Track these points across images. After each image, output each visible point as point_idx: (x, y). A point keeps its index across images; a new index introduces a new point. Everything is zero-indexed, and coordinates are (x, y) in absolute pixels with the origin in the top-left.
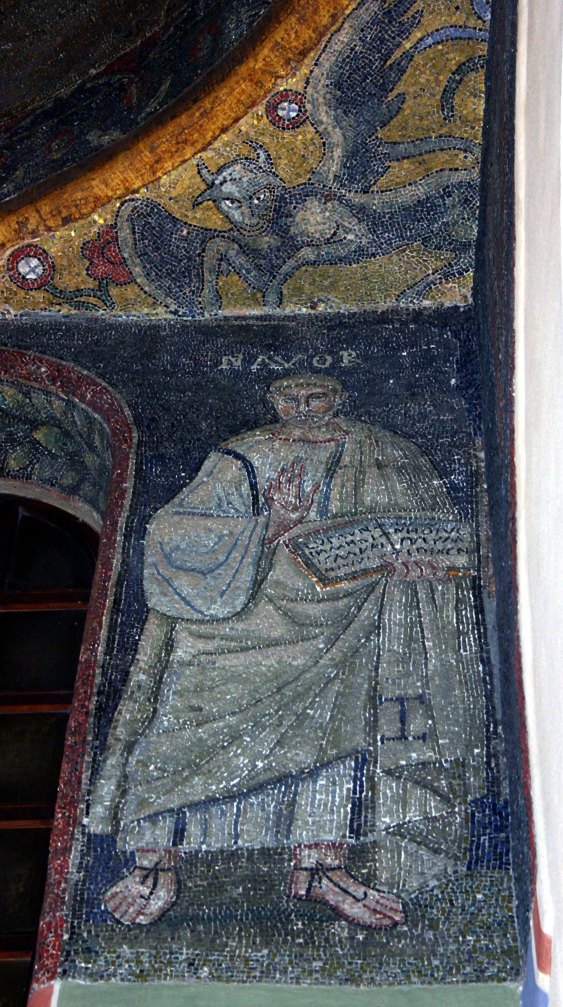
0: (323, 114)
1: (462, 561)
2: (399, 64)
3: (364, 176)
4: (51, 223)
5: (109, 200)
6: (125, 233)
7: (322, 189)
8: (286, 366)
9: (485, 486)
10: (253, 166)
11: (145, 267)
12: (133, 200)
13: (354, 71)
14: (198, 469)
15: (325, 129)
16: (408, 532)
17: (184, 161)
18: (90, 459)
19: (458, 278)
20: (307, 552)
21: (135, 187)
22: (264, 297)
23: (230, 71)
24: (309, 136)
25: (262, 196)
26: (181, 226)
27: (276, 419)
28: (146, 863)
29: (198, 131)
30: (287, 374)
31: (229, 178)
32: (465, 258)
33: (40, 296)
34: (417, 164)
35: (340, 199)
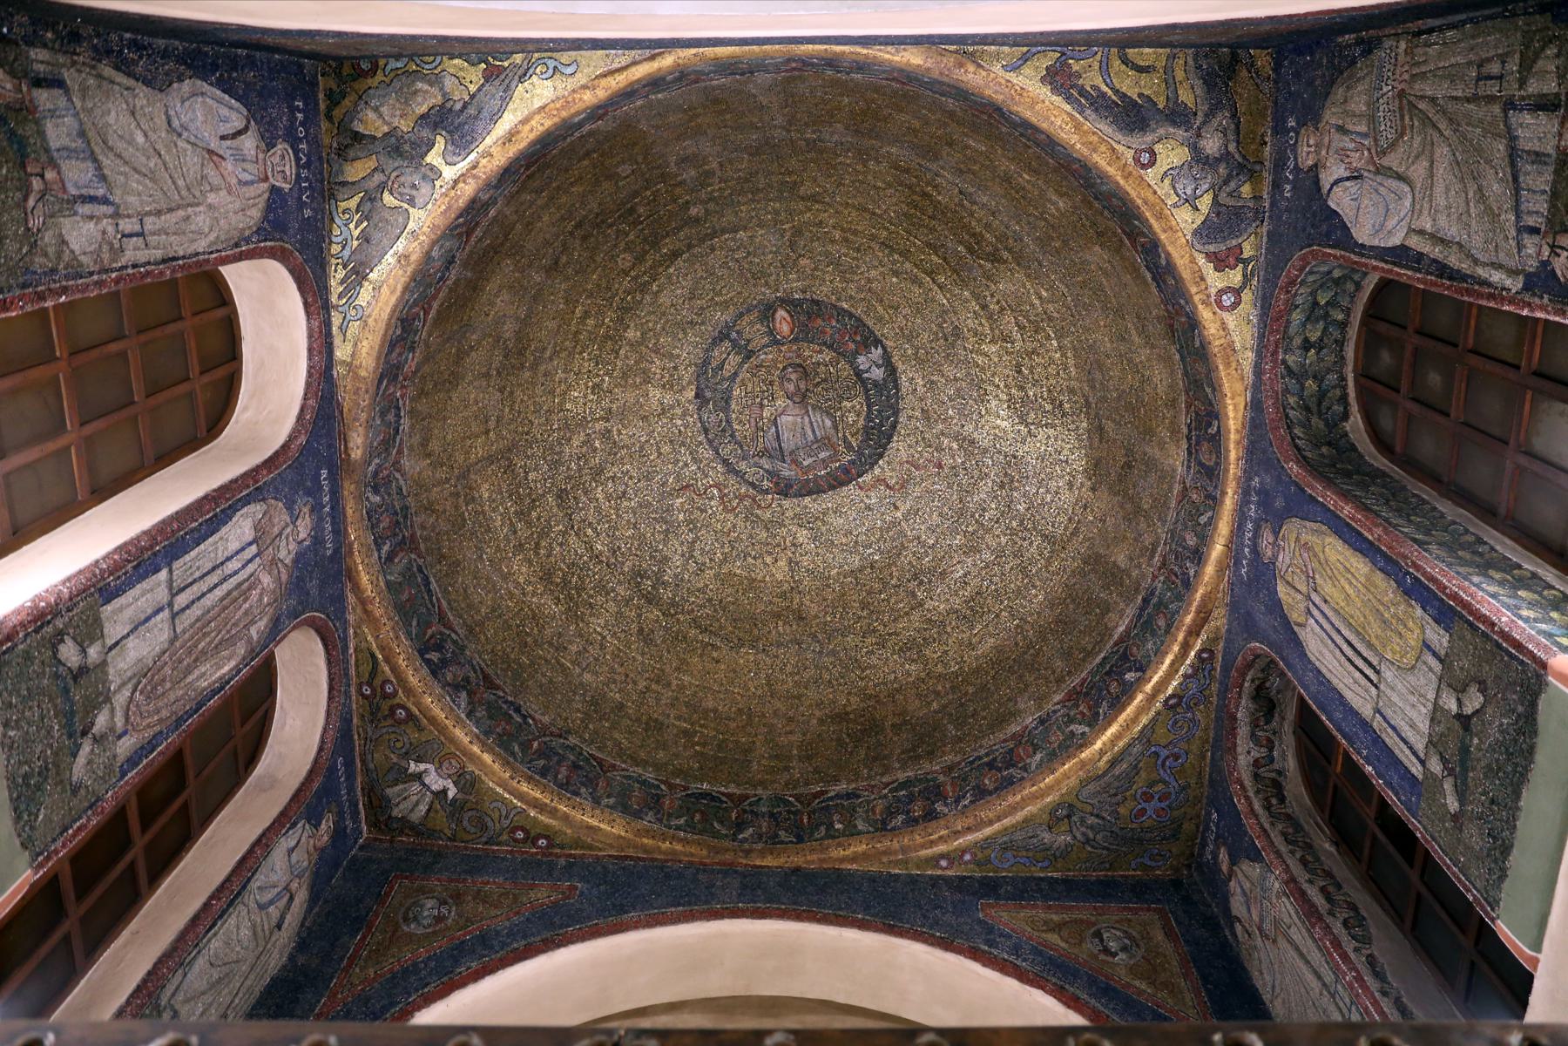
1: (1403, 45)
3: (1186, 116)
5: (1191, 255)
6: (1212, 248)
18: (1337, 274)
27: (1316, 165)
30: (1296, 159)
33: (1247, 296)
35: (1199, 128)
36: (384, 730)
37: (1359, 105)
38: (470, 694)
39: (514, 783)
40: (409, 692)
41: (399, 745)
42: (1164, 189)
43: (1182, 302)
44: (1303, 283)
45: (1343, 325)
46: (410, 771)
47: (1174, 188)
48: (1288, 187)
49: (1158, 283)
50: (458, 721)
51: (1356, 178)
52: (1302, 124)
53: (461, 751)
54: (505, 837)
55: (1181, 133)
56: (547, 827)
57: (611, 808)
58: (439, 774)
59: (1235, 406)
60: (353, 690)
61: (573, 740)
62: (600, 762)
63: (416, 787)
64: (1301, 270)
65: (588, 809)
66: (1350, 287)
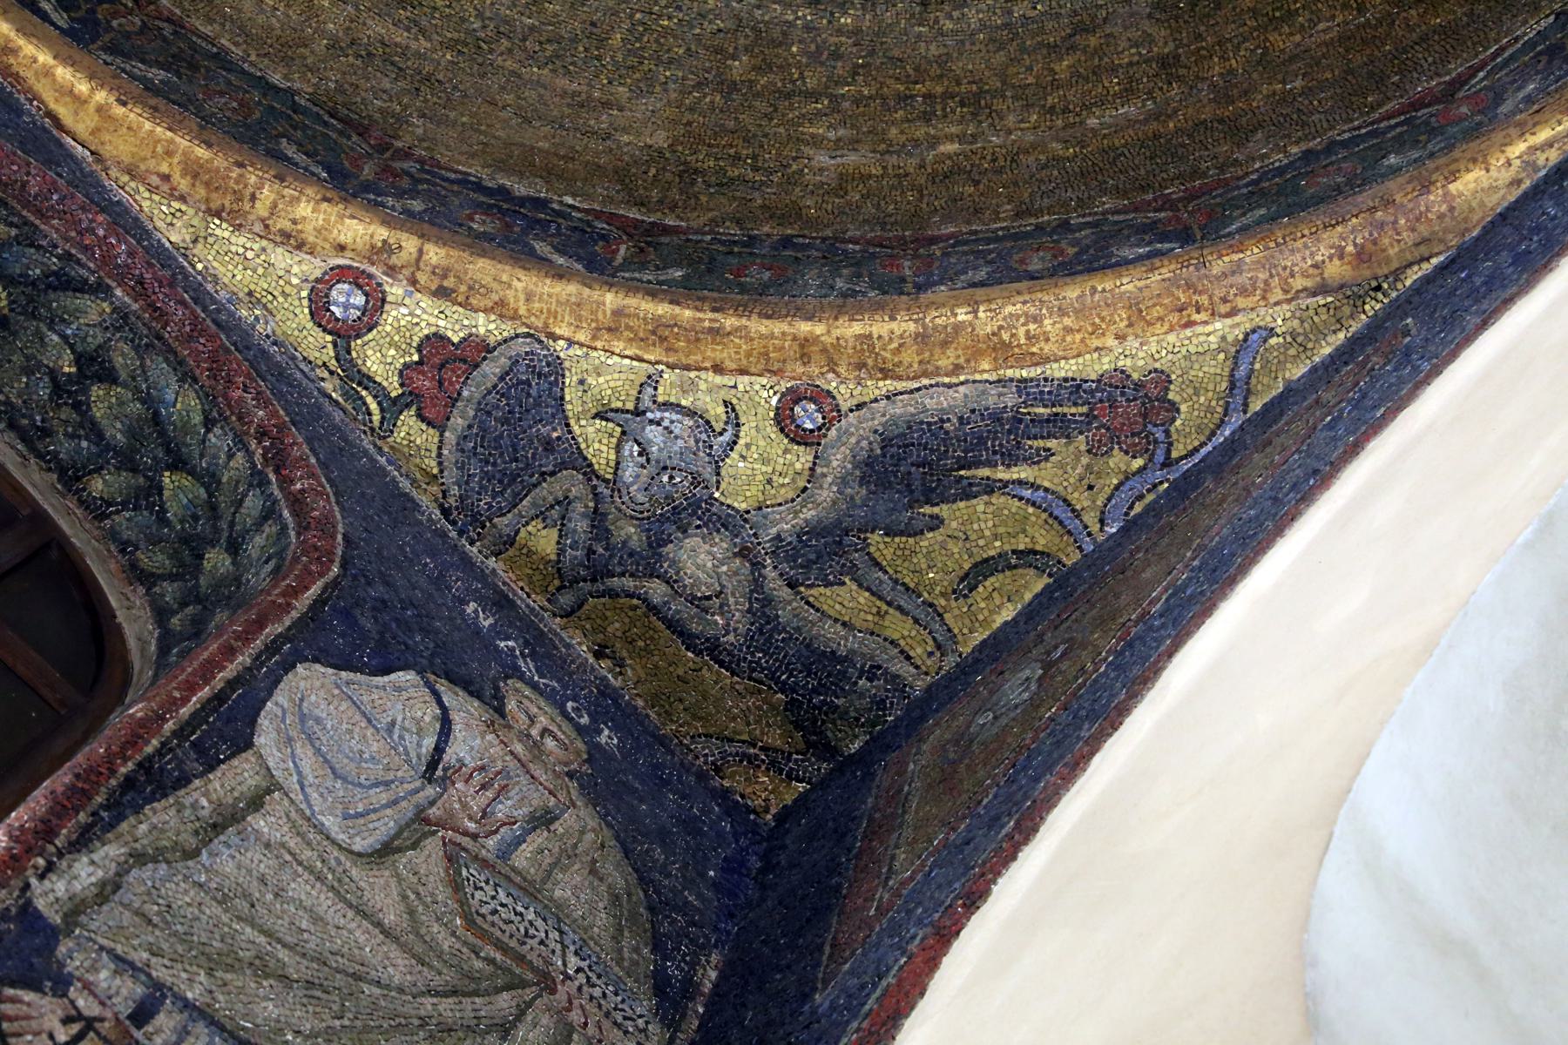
0: (839, 457)
2: (971, 485)
3: (807, 566)
4: (422, 278)
5: (515, 317)
6: (491, 370)
7: (749, 535)
8: (536, 678)
9: (701, 1010)
10: (704, 436)
11: (470, 427)
12: (541, 342)
13: (919, 444)
14: (386, 671)
15: (824, 475)
16: (590, 967)
17: (641, 360)
18: (217, 561)
19: (782, 781)
20: (464, 873)
21: (558, 331)
22: (559, 589)
23: (786, 316)
24: (798, 466)
25: (678, 480)
26: (560, 424)
27: (500, 711)
28: (81, 1003)
29: (688, 341)
30: (534, 686)
31: (666, 423)
32: (812, 765)
33: (316, 345)
34: (874, 610)
35: (757, 565)
37: (567, 888)
42: (707, 394)
43: (417, 205)
44: (258, 480)
45: (71, 477)
47: (690, 413)
48: (486, 623)
49: (489, 192)
51: (433, 764)
52: (596, 754)
55: (786, 524)
59: (80, 101)
64: (297, 503)
66: (155, 560)
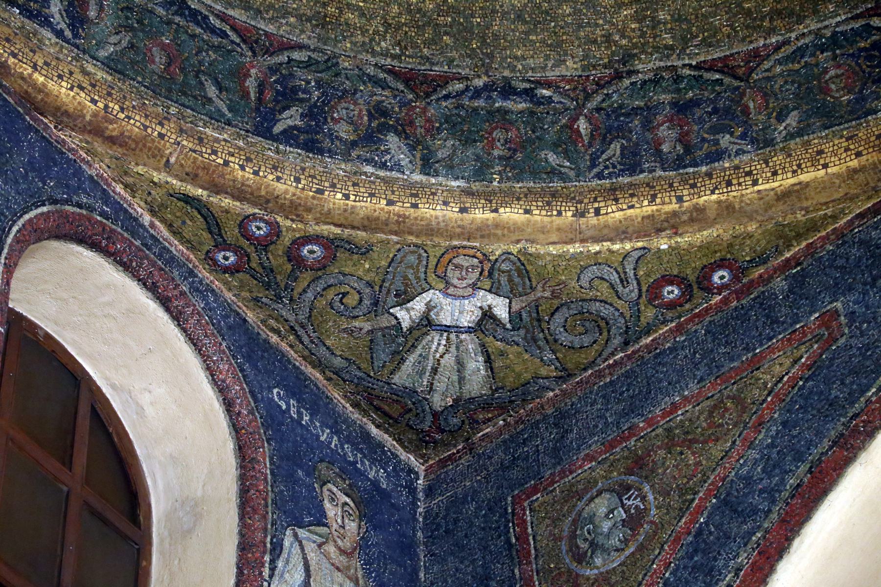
36: (310, 295)
38: (403, 130)
39: (592, 220)
40: (294, 209)
41: (352, 300)
46: (405, 325)
50: (415, 192)
53: (459, 236)
54: (649, 314)
56: (705, 247)
57: (800, 133)
58: (455, 297)
60: (204, 274)
61: (645, 66)
62: (725, 66)
63: (436, 342)
65: (757, 166)
